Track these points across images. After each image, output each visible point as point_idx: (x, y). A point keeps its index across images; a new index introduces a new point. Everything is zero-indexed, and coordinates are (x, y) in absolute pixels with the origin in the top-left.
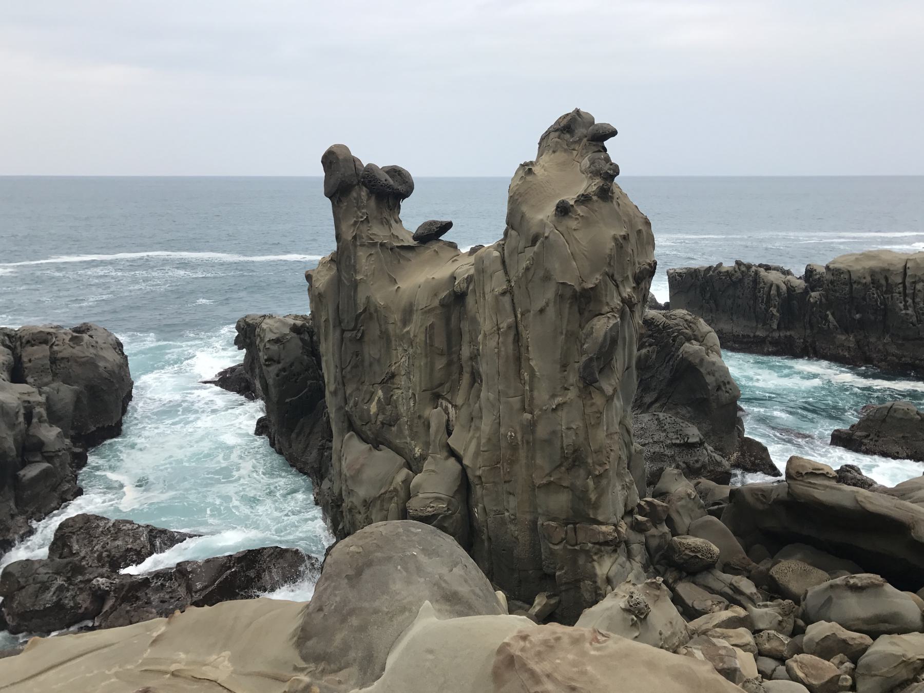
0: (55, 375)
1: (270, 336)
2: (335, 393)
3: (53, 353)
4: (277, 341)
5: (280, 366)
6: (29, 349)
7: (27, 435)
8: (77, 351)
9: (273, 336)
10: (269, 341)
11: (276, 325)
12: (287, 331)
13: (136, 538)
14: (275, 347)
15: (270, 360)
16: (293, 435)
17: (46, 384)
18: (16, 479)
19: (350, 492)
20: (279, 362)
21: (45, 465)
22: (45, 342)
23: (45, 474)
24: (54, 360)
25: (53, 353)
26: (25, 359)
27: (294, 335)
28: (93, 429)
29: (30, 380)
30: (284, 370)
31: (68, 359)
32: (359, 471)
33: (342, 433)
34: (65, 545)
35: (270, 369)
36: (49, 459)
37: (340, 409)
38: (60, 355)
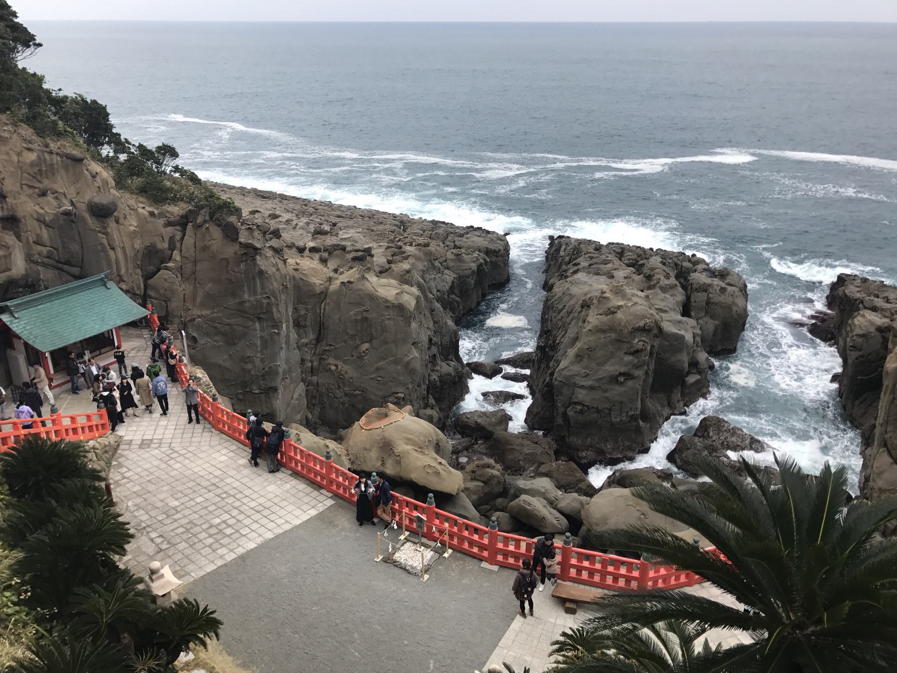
0: (707, 312)
1: (858, 331)
2: (881, 425)
3: (708, 298)
4: (863, 336)
5: (860, 353)
6: (696, 293)
7: (693, 358)
8: (722, 299)
9: (861, 332)
10: (857, 335)
11: (866, 323)
12: (872, 330)
13: (743, 441)
14: (860, 340)
15: (854, 347)
16: (857, 402)
17: (701, 318)
18: (684, 381)
19: (874, 480)
20: (860, 350)
21: (698, 377)
22: (706, 291)
23: (698, 382)
24: (708, 303)
25: (708, 298)
26: (693, 300)
27: (878, 333)
28: (720, 348)
29: (693, 314)
30: (863, 356)
31: (716, 304)
32: (881, 473)
33: (879, 446)
34: (706, 430)
35: (852, 353)
36: (699, 373)
37: (881, 434)
38: (712, 300)
